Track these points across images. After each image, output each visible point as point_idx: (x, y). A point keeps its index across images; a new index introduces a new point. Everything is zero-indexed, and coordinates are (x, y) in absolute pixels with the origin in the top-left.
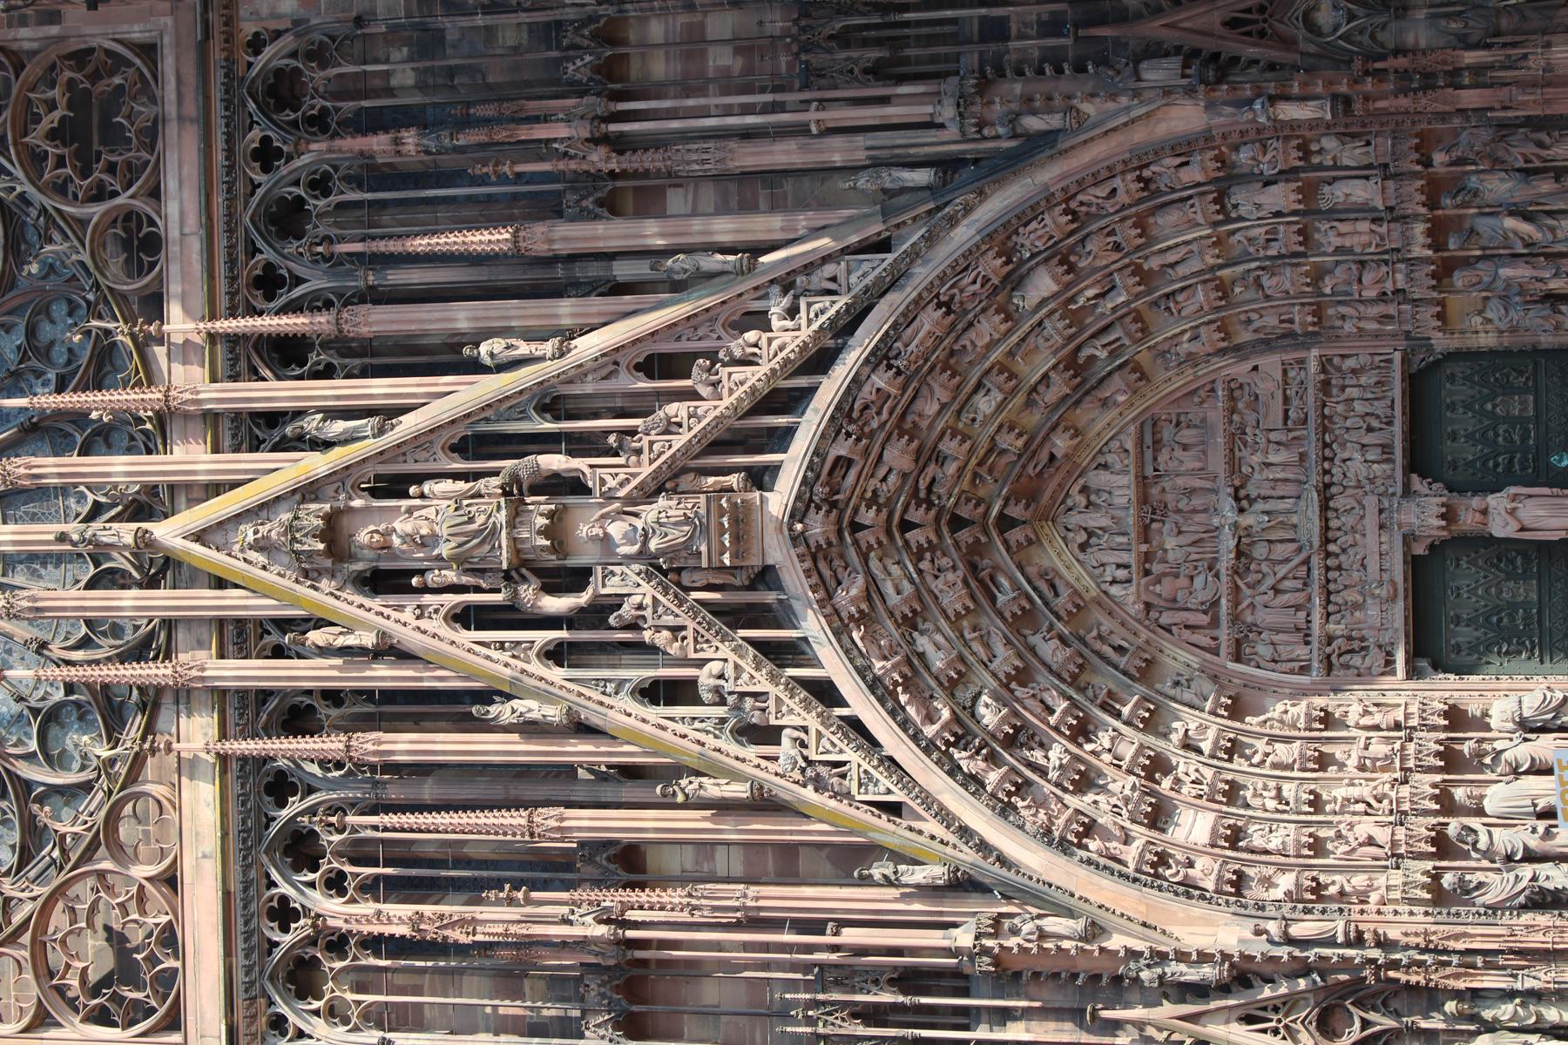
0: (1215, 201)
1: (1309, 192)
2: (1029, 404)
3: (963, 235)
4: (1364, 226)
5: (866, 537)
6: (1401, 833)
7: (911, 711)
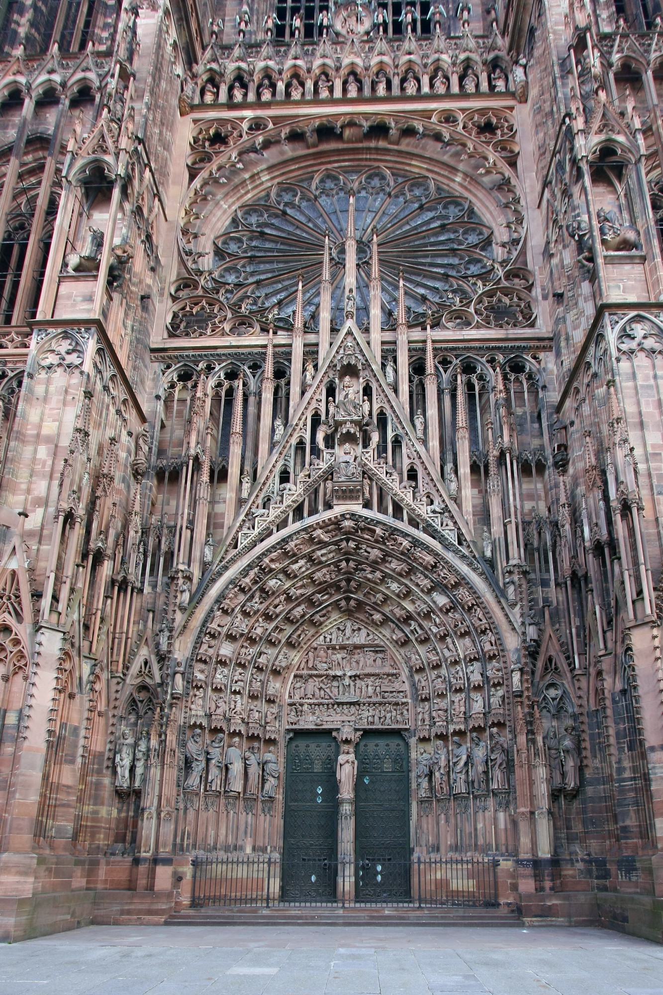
1: (478, 688)
5: (344, 544)
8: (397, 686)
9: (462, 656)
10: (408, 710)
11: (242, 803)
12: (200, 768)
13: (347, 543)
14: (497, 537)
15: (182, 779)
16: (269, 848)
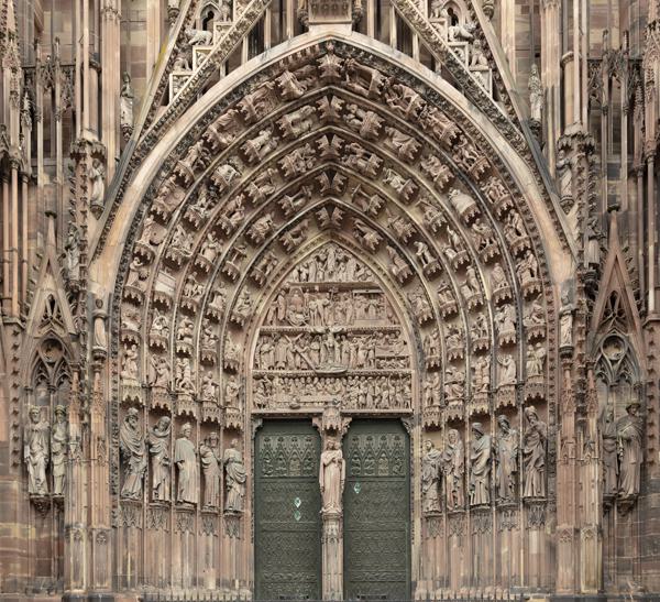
0: (507, 297)
1: (509, 347)
8: (396, 348)
9: (488, 297)
10: (410, 386)
11: (199, 519)
12: (142, 466)
13: (330, 100)
14: (550, 86)
15: (117, 483)
16: (237, 582)
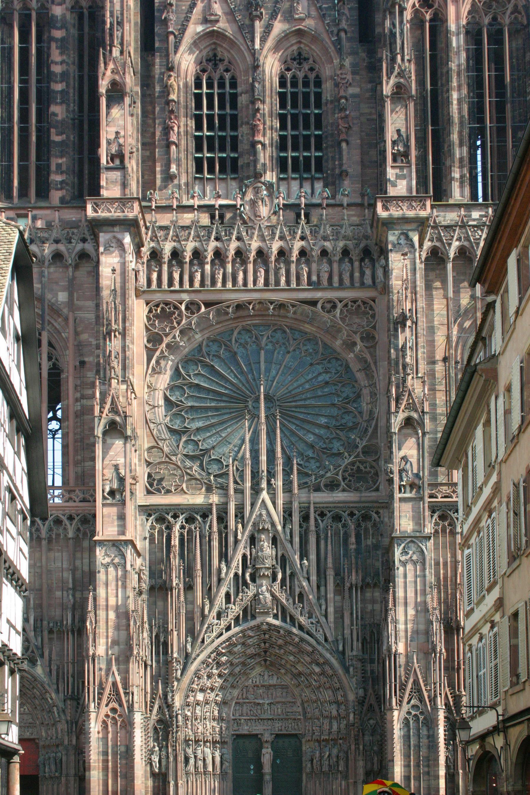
1: (335, 718)
2: (292, 666)
3: (328, 656)
4: (328, 727)
5: (262, 636)
6: (200, 734)
7: (224, 645)
